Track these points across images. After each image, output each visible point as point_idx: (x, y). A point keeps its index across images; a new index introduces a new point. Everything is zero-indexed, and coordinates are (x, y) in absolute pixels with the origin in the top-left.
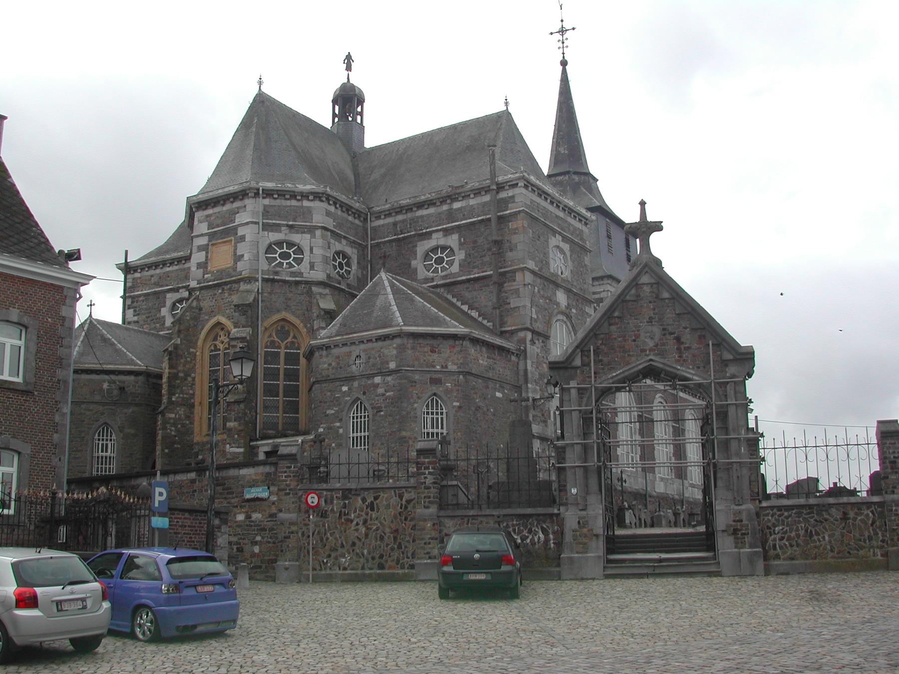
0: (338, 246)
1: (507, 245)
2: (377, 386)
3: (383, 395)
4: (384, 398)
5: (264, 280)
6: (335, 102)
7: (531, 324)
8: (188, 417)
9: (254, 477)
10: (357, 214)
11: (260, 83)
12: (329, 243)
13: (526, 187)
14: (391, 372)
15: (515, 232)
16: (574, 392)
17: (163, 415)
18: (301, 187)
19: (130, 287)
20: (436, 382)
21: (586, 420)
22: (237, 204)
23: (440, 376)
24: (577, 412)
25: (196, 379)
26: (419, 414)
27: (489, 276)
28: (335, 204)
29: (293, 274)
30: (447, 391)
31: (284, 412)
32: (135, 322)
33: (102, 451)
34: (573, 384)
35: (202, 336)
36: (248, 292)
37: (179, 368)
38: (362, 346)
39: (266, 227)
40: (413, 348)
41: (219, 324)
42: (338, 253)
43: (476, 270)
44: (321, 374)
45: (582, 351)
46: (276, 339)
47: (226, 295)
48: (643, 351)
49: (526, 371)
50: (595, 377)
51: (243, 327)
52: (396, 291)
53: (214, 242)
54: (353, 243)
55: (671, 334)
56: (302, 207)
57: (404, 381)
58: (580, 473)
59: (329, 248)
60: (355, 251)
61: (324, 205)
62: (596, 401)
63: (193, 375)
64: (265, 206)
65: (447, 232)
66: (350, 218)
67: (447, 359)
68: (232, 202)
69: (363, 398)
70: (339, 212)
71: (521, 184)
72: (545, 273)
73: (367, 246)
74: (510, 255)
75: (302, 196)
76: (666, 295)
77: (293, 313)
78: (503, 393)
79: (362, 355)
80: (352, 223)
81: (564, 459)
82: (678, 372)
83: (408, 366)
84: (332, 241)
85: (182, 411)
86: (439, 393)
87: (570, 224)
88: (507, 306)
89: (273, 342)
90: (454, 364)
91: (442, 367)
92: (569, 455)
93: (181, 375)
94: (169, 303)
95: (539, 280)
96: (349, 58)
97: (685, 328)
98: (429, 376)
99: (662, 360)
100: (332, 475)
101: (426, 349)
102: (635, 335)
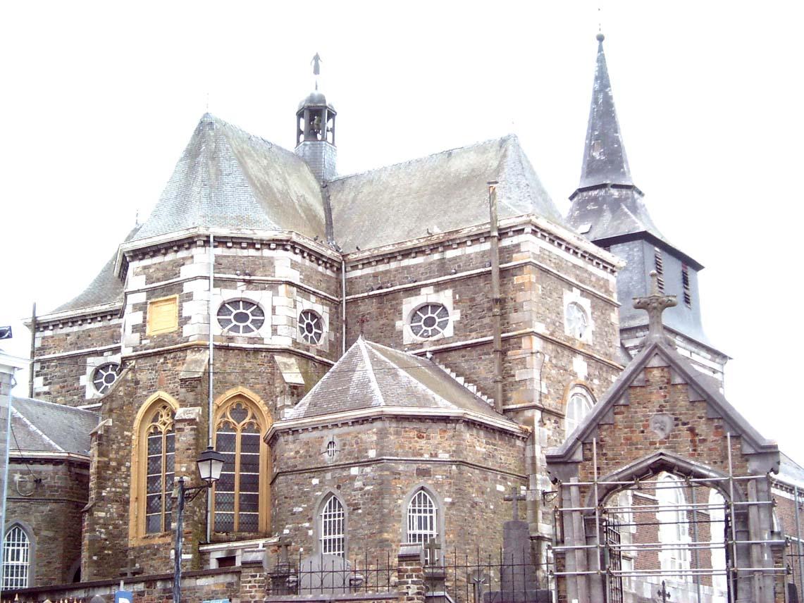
0: (307, 304)
1: (510, 304)
2: (353, 478)
3: (361, 489)
4: (360, 493)
5: (217, 348)
6: (300, 115)
7: (540, 400)
8: (121, 516)
9: (213, 588)
10: (329, 263)
12: (295, 301)
13: (534, 232)
14: (370, 462)
15: (520, 288)
16: (574, 490)
17: (92, 515)
19: (39, 349)
20: (423, 473)
21: (589, 523)
22: (183, 254)
23: (429, 466)
24: (578, 513)
25: (132, 469)
26: (404, 511)
27: (490, 342)
28: (302, 252)
29: (252, 340)
30: (438, 485)
31: (241, 510)
32: (46, 393)
33: (13, 560)
34: (573, 481)
35: (139, 416)
36: (197, 363)
37: (111, 456)
38: (336, 431)
39: (219, 283)
40: (397, 433)
41: (160, 400)
42: (305, 313)
43: (473, 334)
44: (286, 463)
45: (584, 444)
46: (231, 420)
47: (170, 365)
48: (653, 443)
49: (534, 458)
50: (599, 473)
51: (191, 406)
52: (375, 362)
53: (153, 300)
54: (324, 299)
55: (684, 424)
56: (262, 257)
57: (386, 473)
58: (581, 582)
59: (295, 307)
60: (327, 309)
61: (290, 254)
62: (600, 501)
63: (128, 464)
64: (217, 257)
65: (439, 287)
66: (321, 269)
67: (438, 445)
68: (176, 251)
69: (337, 492)
70: (307, 262)
71: (528, 229)
72: (559, 337)
73: (340, 302)
74: (514, 317)
75: (262, 244)
76: (678, 380)
77: (252, 388)
78: (506, 486)
79: (336, 440)
80: (323, 275)
81: (564, 566)
82: (693, 468)
83: (391, 455)
84: (299, 298)
85: (114, 508)
86: (426, 486)
87: (591, 274)
88: (510, 379)
89: (227, 423)
91: (431, 455)
92: (569, 561)
93: (113, 464)
94: (90, 370)
95: (550, 347)
97: (700, 418)
98: (415, 466)
99: (674, 455)
100: (303, 584)
101: (411, 435)
102: (644, 426)
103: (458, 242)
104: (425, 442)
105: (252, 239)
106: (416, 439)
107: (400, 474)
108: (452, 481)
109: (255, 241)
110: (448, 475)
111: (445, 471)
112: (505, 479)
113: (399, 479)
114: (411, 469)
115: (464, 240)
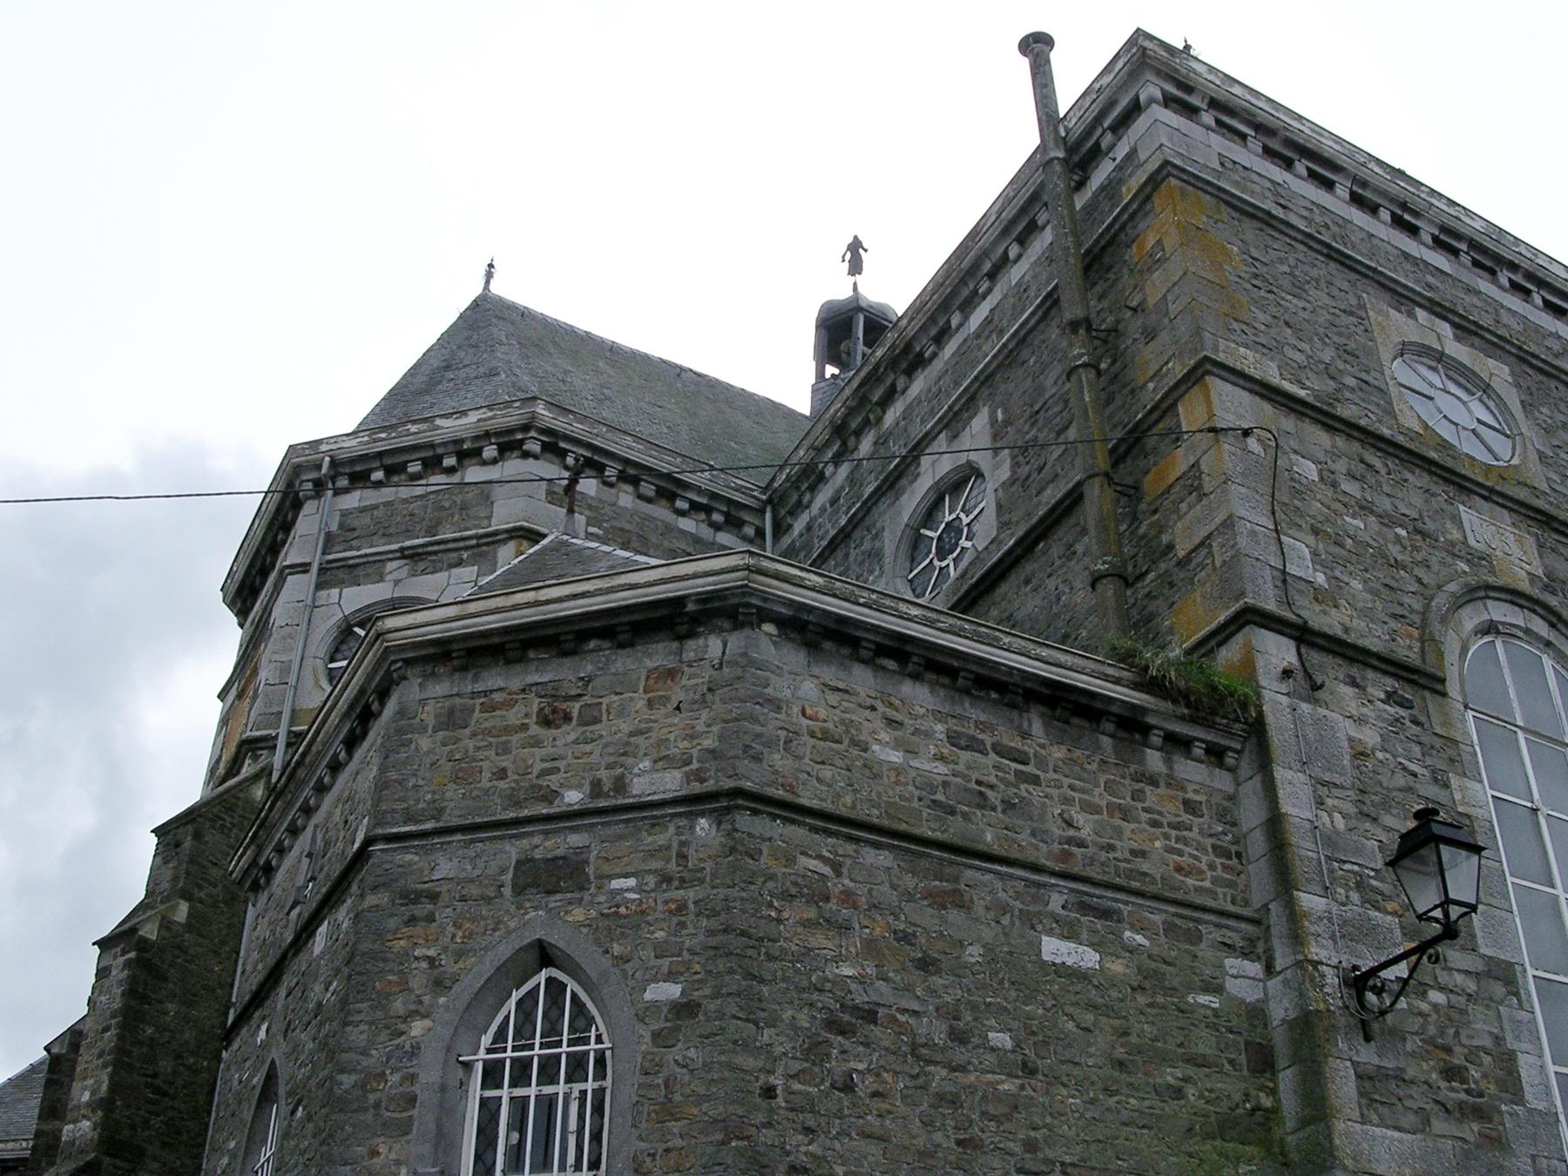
1: (1134, 326)
11: (489, 276)
18: (450, 427)
49: (1275, 824)
64: (345, 514)
83: (410, 818)
86: (555, 938)
90: (664, 761)
96: (855, 247)
101: (514, 716)
103: (987, 266)
104: (573, 737)
105: (432, 446)
106: (535, 729)
107: (434, 897)
108: (691, 894)
109: (440, 451)
110: (673, 867)
111: (651, 854)
112: (1105, 914)
113: (430, 918)
114: (493, 867)
115: (1001, 250)
